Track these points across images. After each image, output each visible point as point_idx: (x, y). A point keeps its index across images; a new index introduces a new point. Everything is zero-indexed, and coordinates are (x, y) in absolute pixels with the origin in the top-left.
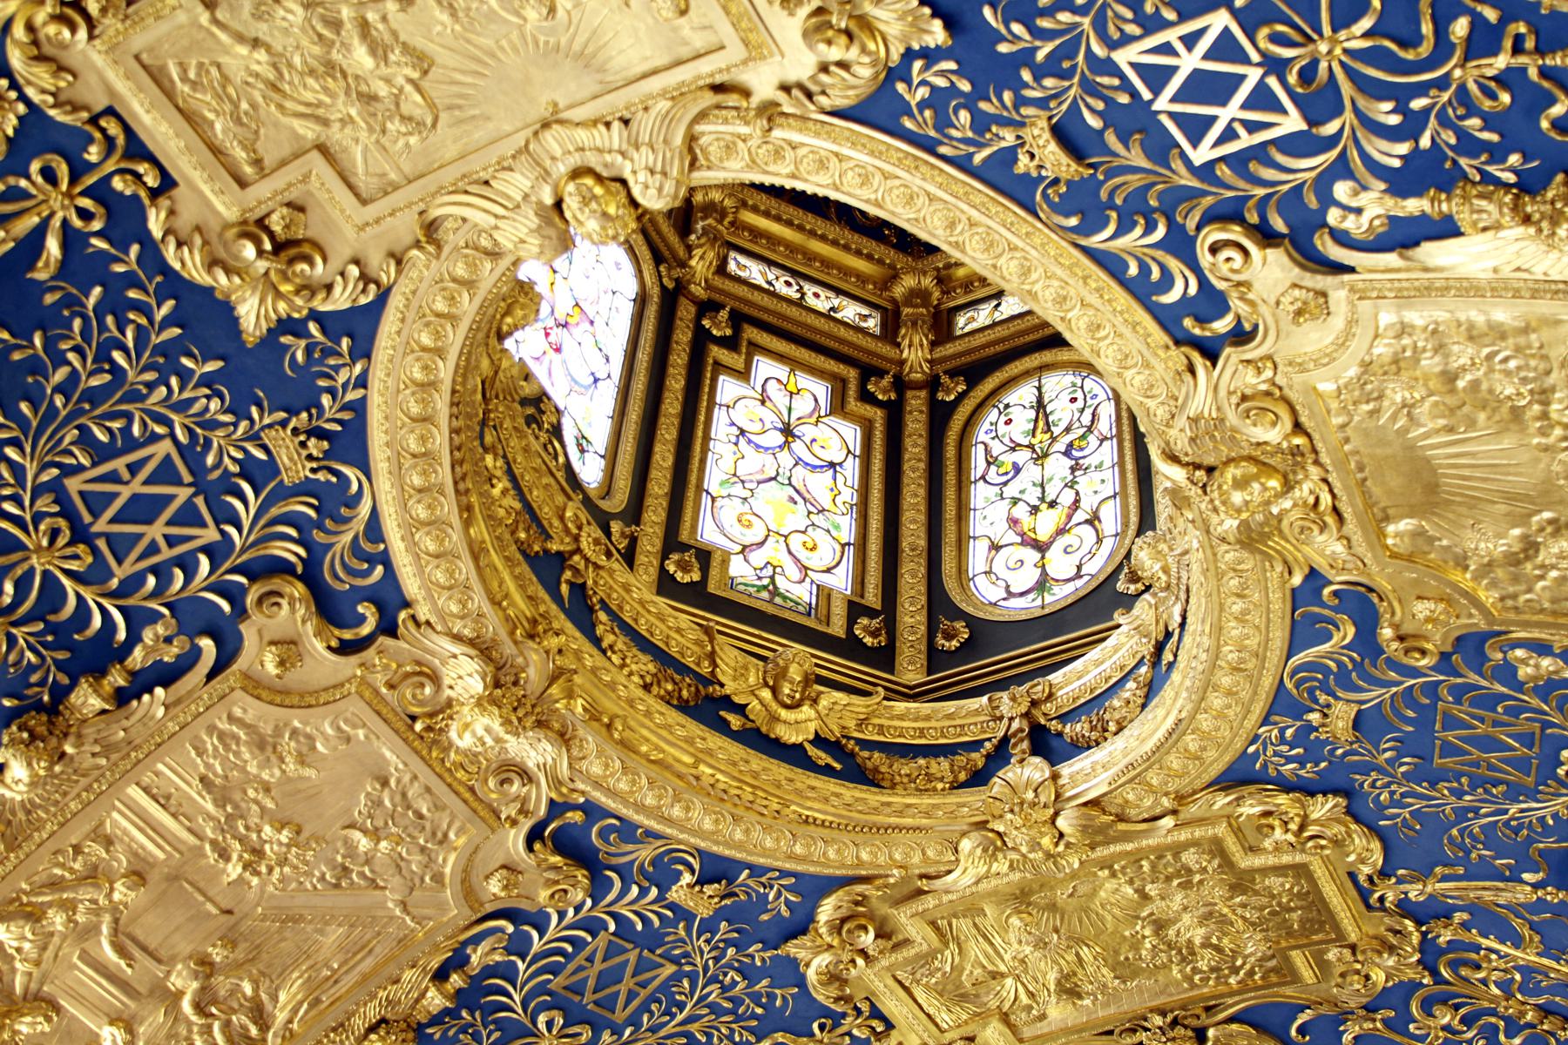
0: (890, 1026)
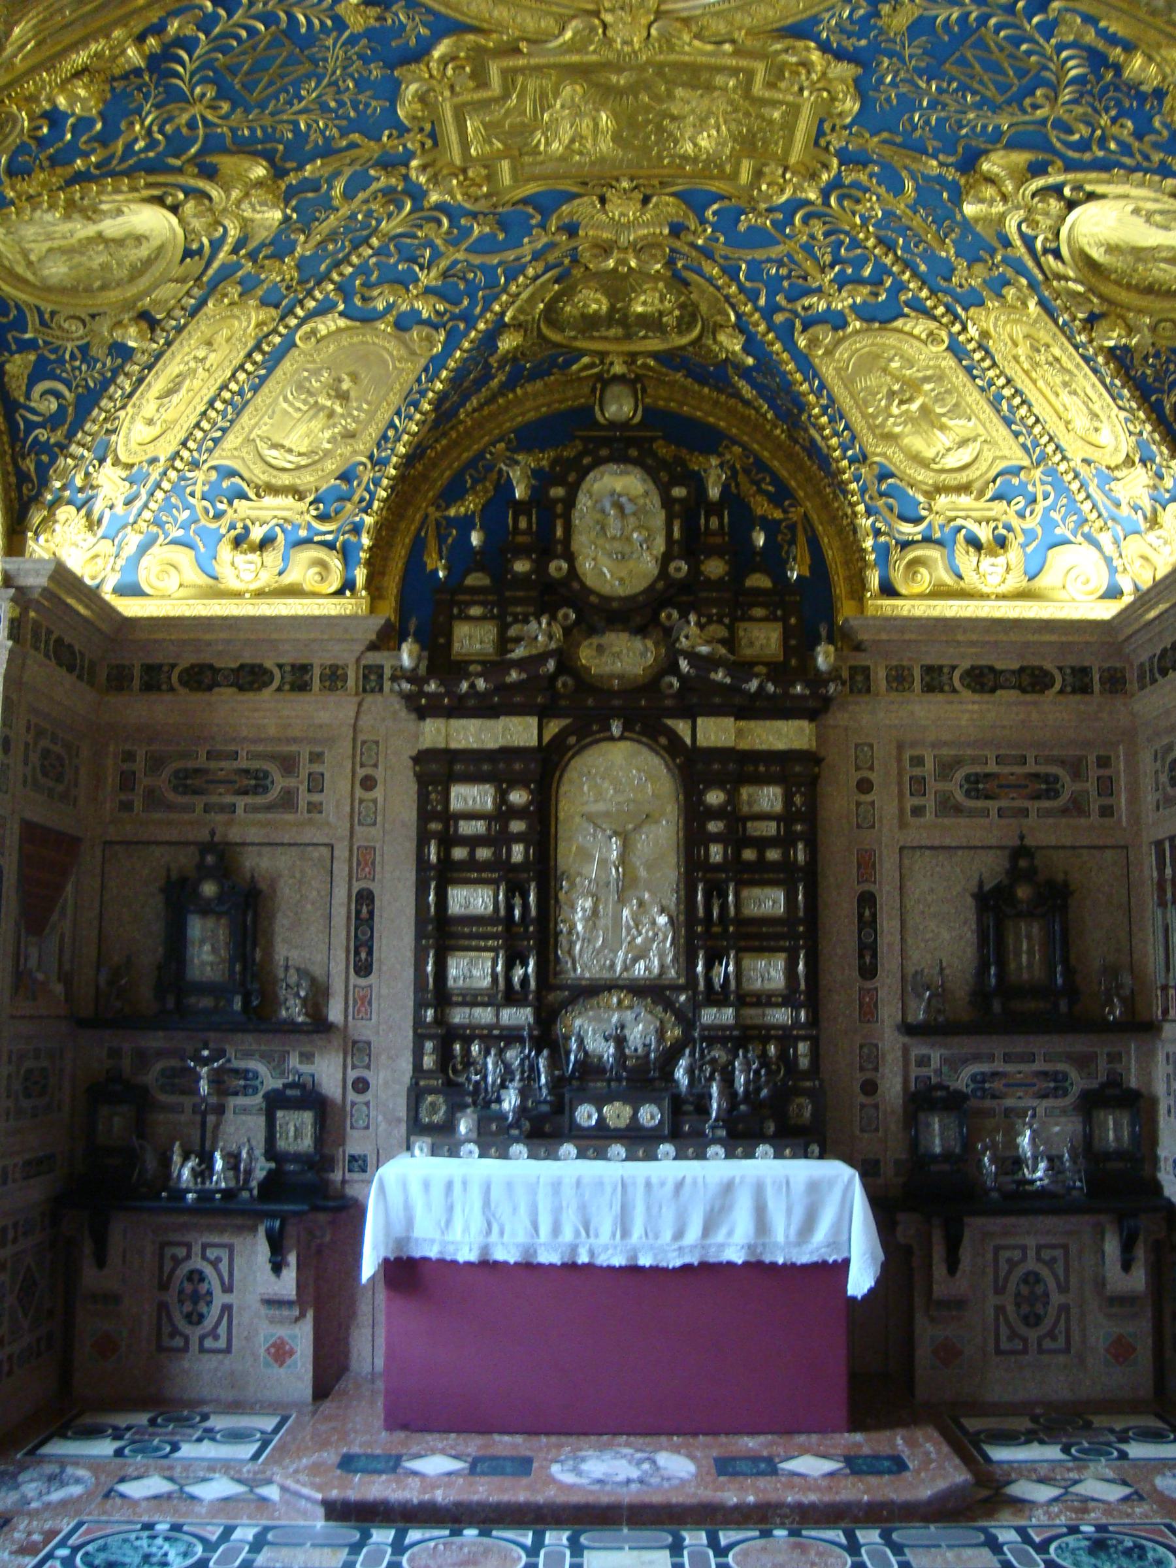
0: (436, 144)
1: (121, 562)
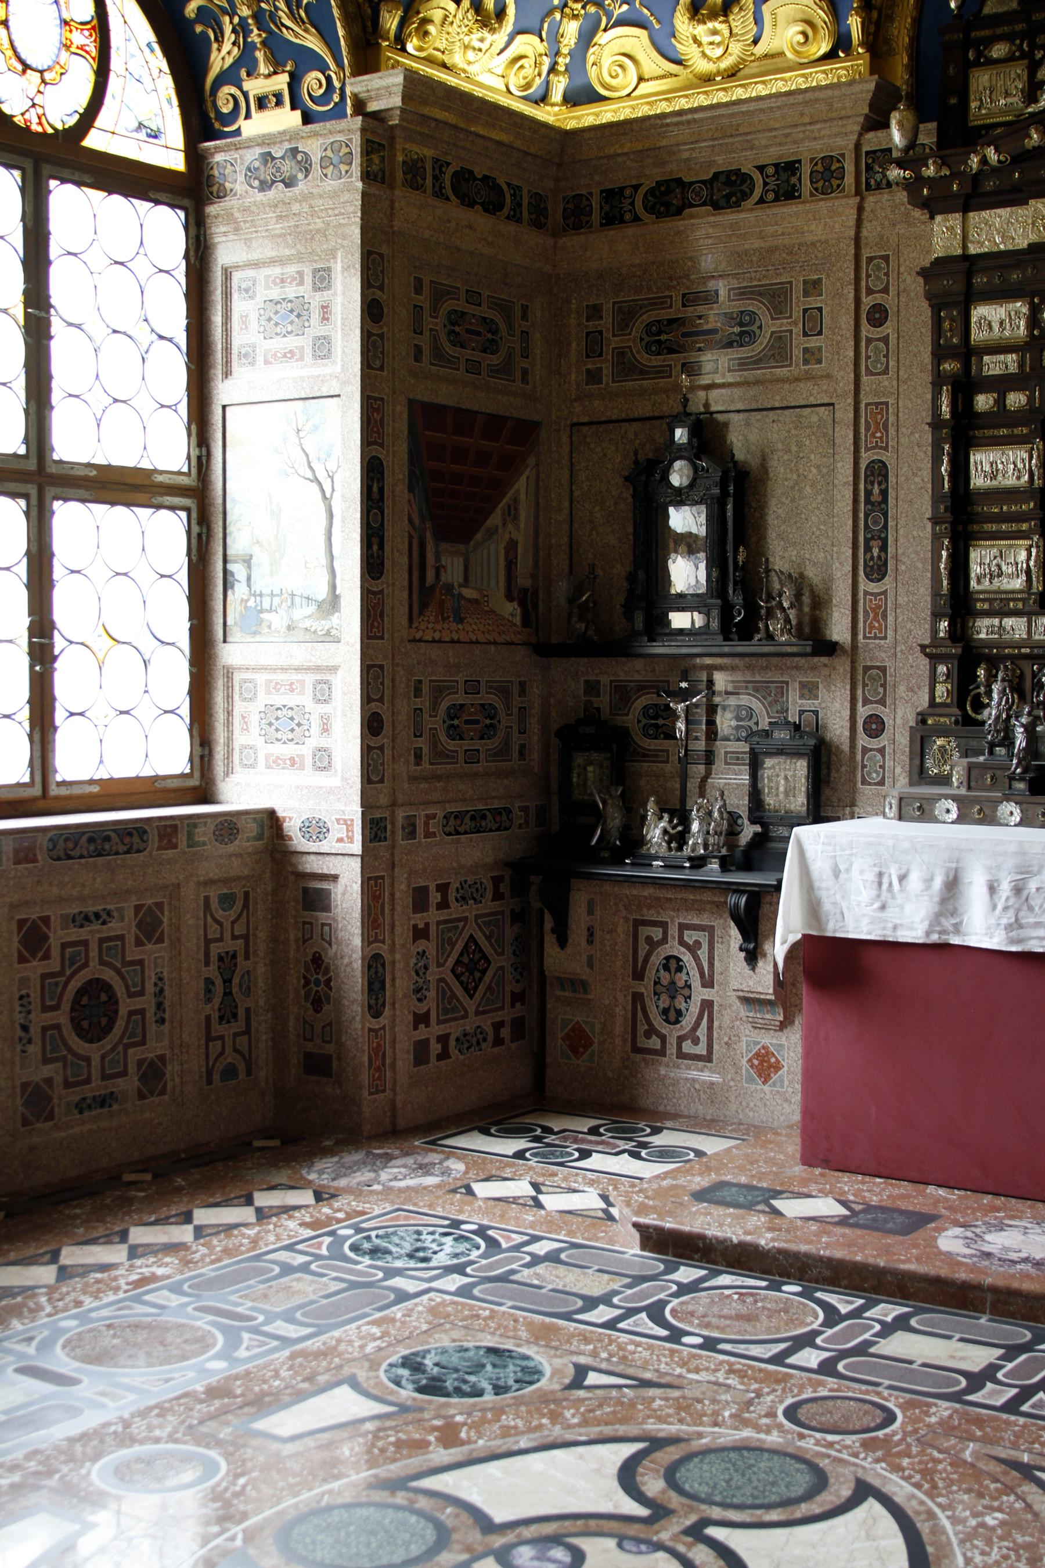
1: (563, 61)
